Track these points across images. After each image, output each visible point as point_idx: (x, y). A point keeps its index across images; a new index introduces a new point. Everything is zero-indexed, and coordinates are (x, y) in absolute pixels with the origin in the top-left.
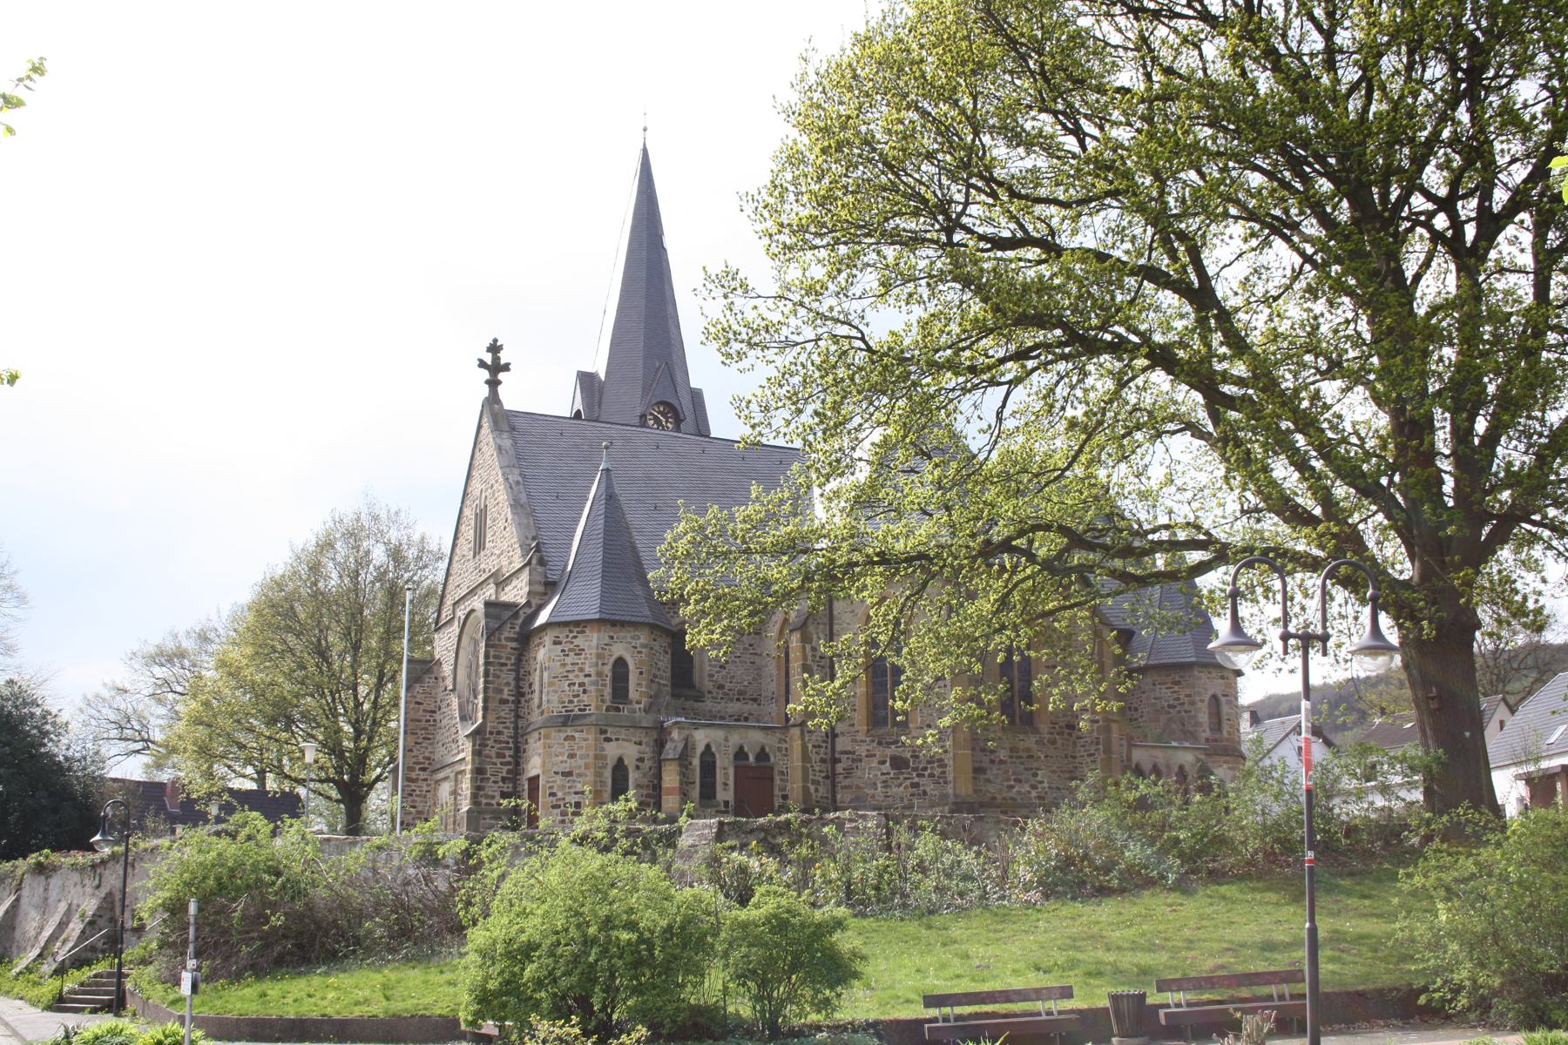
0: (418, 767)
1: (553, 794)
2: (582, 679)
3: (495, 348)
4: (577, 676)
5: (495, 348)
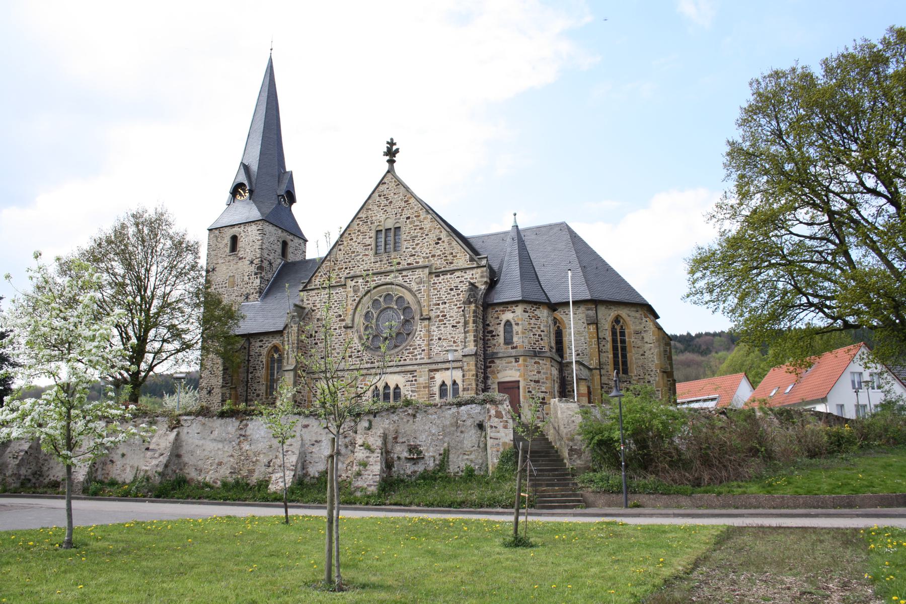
1: (530, 392)
2: (539, 333)
3: (392, 143)
5: (392, 143)
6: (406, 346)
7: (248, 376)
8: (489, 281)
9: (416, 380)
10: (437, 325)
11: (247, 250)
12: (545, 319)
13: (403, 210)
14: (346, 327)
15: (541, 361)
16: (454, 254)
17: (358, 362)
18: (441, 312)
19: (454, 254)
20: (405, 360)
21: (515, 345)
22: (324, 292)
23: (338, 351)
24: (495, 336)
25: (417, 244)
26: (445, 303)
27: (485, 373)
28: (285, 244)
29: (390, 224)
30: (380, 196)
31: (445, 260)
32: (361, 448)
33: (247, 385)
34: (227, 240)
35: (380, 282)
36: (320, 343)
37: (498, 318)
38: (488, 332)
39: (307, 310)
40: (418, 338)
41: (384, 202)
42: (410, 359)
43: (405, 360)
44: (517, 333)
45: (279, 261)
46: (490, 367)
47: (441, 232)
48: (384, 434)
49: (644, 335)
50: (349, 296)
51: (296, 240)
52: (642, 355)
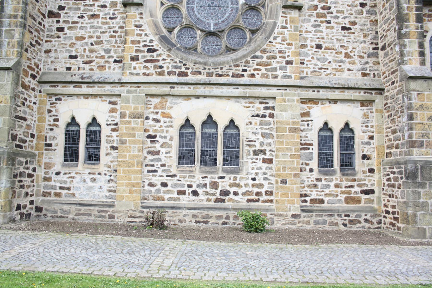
0: (30, 72)
6: (255, 51)
9: (272, 116)
10: (312, 23)
17: (152, 71)
20: (253, 76)
23: (106, 46)
36: (70, 28)
40: (279, 40)
42: (263, 76)
43: (253, 76)
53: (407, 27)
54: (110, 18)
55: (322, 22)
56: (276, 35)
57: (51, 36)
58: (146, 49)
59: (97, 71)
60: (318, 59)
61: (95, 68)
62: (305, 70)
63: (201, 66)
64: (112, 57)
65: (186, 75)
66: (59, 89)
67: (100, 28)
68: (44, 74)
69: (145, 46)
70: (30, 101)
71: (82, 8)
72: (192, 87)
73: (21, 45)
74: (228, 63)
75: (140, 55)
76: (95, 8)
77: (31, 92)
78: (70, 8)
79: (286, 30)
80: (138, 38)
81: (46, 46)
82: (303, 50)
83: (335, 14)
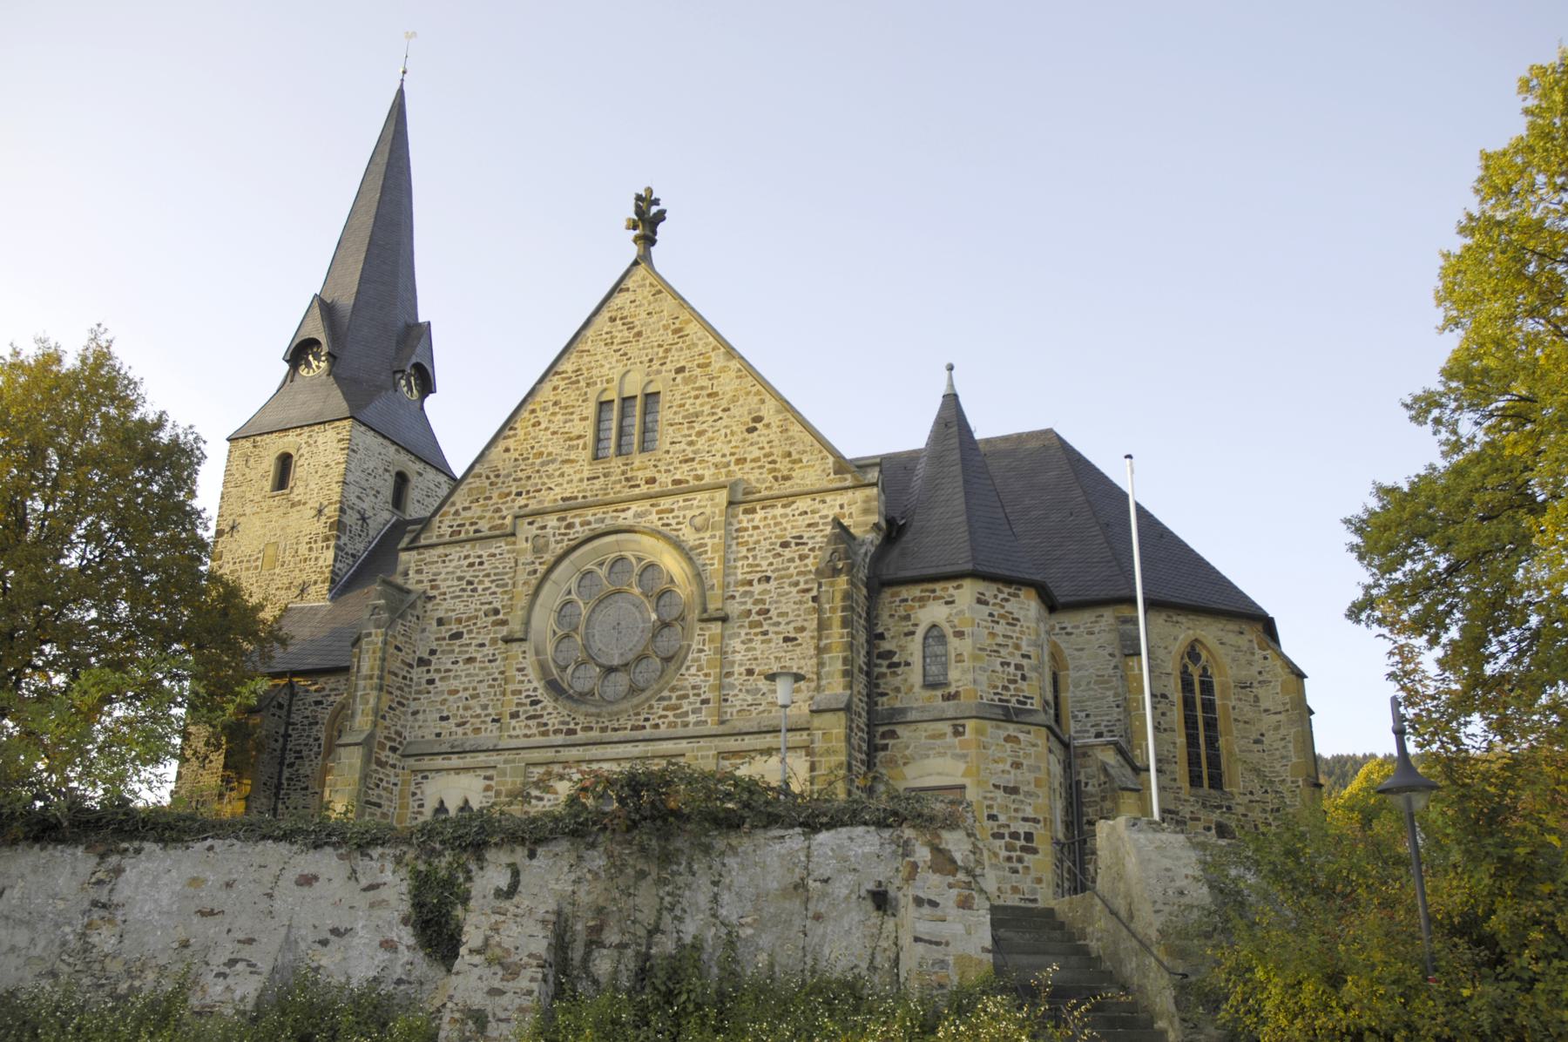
0: (389, 744)
1: (992, 817)
2: (1019, 660)
4: (1011, 654)
7: (281, 772)
8: (883, 525)
10: (743, 637)
11: (312, 486)
12: (1033, 625)
13: (667, 351)
14: (507, 640)
15: (1022, 736)
16: (795, 456)
17: (534, 730)
18: (756, 602)
19: (795, 456)
20: (657, 726)
21: (952, 690)
22: (455, 552)
23: (484, 700)
24: (897, 665)
25: (700, 434)
26: (768, 579)
27: (870, 764)
28: (402, 480)
29: (634, 386)
30: (613, 320)
31: (771, 471)
32: (477, 959)
33: (277, 795)
34: (269, 464)
35: (602, 527)
36: (442, 679)
37: (907, 618)
38: (881, 656)
39: (412, 597)
40: (693, 670)
41: (621, 333)
44: (960, 658)
45: (386, 515)
46: (885, 747)
47: (763, 401)
48: (559, 913)
49: (1261, 692)
50: (520, 562)
51: (431, 474)
52: (1257, 742)
53: (827, 638)
54: (490, 661)
55: (756, 634)
56: (689, 663)
57: (419, 692)
58: (528, 701)
59: (471, 736)
60: (748, 691)
61: (469, 732)
62: (729, 710)
63: (593, 719)
64: (489, 715)
65: (571, 732)
66: (426, 763)
67: (477, 675)
68: (410, 743)
69: (528, 697)
70: (388, 782)
71: (457, 650)
72: (581, 749)
73: (376, 711)
74: (626, 711)
75: (521, 709)
76: (472, 649)
77: (389, 770)
78: (443, 652)
79: (702, 655)
80: (518, 687)
81: (414, 706)
82: (728, 680)
83: (775, 619)
